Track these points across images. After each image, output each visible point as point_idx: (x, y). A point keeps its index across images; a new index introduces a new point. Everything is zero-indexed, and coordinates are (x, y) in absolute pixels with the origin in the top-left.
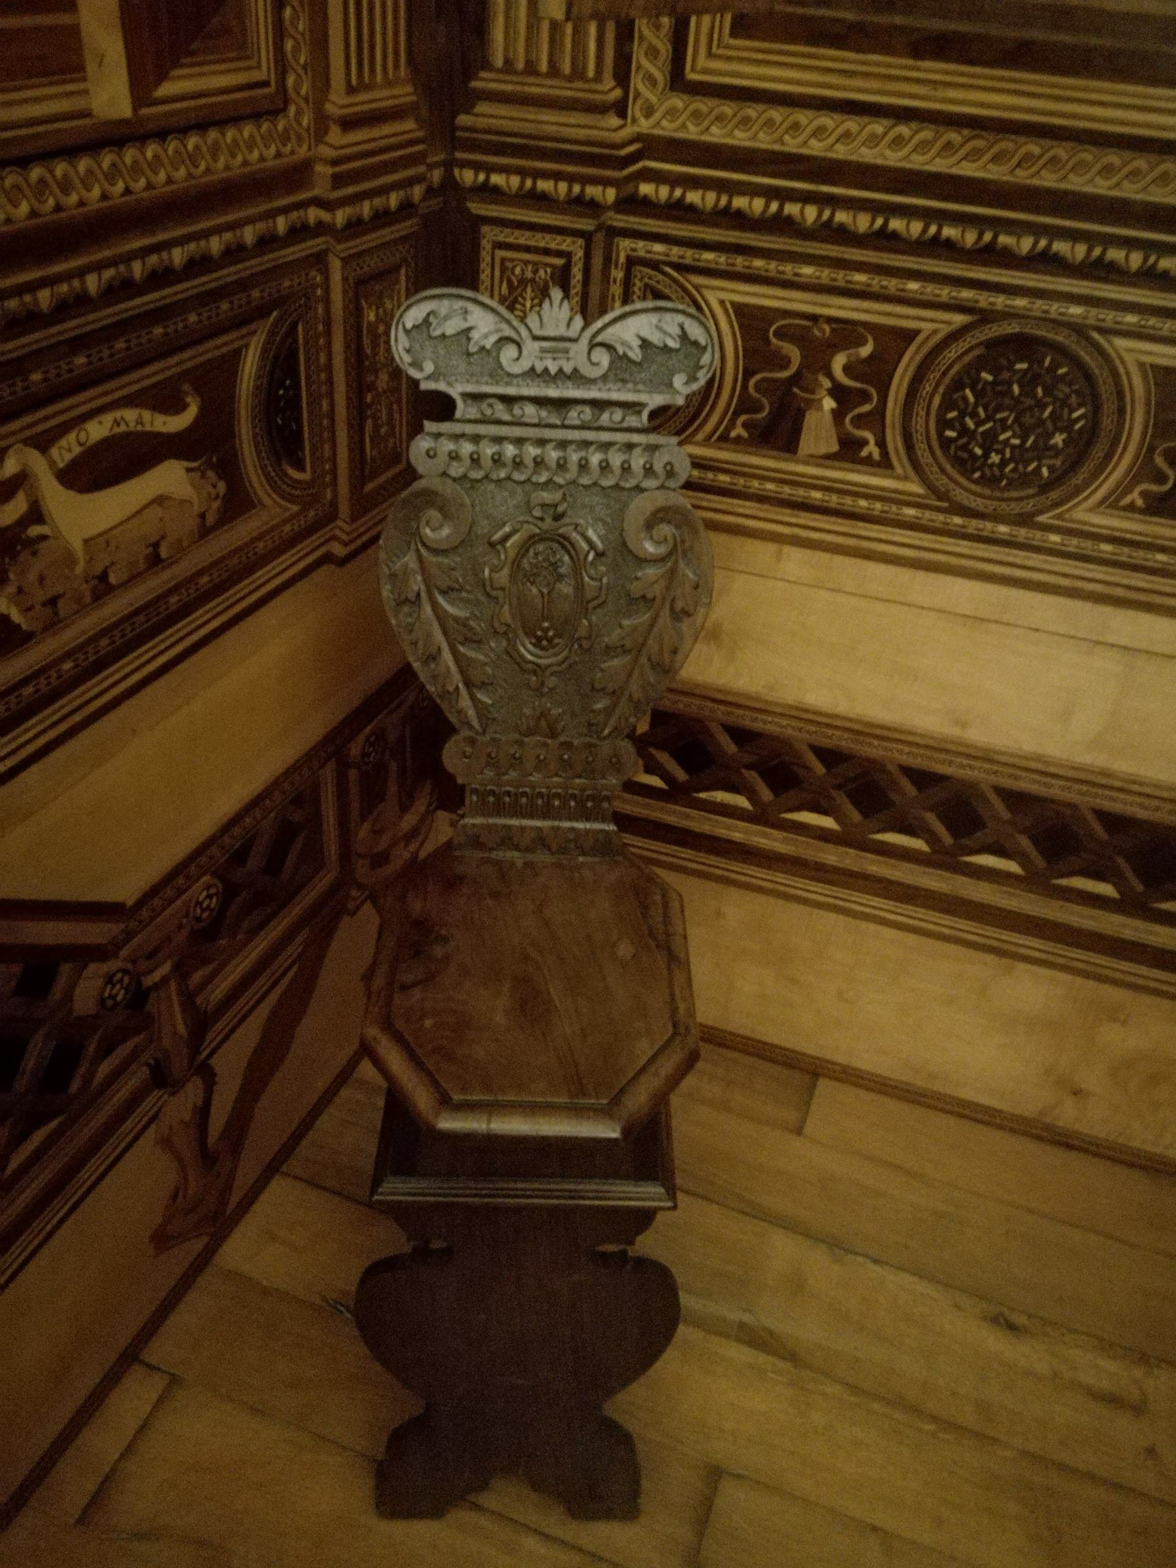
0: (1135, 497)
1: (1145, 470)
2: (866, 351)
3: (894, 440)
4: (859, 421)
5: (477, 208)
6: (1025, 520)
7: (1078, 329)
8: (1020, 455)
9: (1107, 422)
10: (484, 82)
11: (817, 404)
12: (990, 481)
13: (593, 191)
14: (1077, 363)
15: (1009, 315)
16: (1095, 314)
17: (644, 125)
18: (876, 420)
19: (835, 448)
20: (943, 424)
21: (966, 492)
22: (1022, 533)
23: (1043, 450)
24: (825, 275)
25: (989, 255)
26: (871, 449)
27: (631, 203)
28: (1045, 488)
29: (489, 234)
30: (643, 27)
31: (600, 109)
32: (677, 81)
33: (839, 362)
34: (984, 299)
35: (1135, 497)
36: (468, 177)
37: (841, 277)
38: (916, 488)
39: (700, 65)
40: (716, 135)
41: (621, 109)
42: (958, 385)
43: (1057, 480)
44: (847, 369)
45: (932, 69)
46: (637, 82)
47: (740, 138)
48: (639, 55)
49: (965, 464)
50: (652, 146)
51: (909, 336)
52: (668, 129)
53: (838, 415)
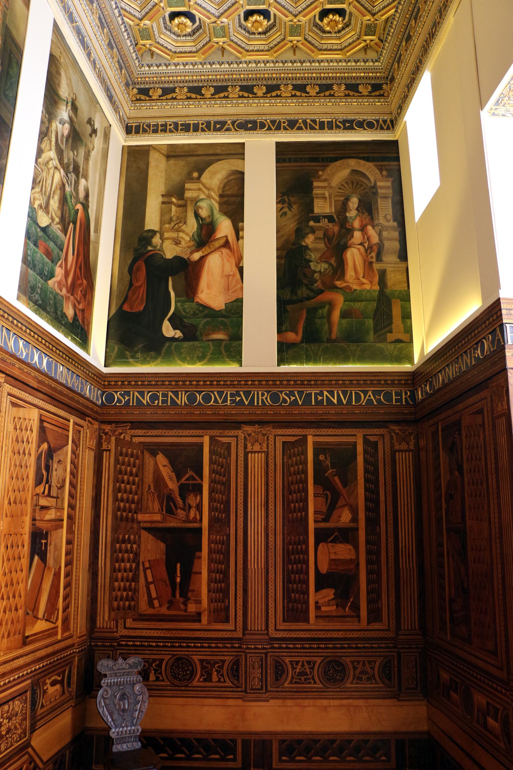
0: (201, 679)
1: (202, 675)
2: (158, 662)
3: (164, 676)
4: (158, 674)
5: (94, 648)
6: (186, 686)
7: (187, 655)
8: (184, 676)
9: (195, 668)
10: (96, 630)
11: (151, 672)
12: (179, 681)
13: (114, 644)
14: (189, 661)
15: (177, 655)
16: (189, 653)
17: (121, 634)
18: (161, 673)
19: (155, 679)
20: (171, 672)
21: (176, 682)
22: (187, 688)
23: (187, 674)
24: (150, 652)
25: (172, 647)
26: (161, 678)
27: (119, 645)
28: (189, 680)
29: (96, 652)
30: (119, 621)
31: (113, 632)
32: (125, 628)
33: (154, 665)
34: (173, 653)
35: (201, 679)
36: (93, 644)
37: (152, 652)
38: (169, 683)
39: (128, 625)
40: (131, 634)
41: (117, 632)
42: (172, 666)
43: (190, 678)
44: (155, 666)
45: (160, 623)
46: (119, 628)
47: (135, 634)
48: (119, 624)
49: (176, 678)
50: (122, 637)
51: (163, 660)
52: (124, 634)
53: (155, 673)
